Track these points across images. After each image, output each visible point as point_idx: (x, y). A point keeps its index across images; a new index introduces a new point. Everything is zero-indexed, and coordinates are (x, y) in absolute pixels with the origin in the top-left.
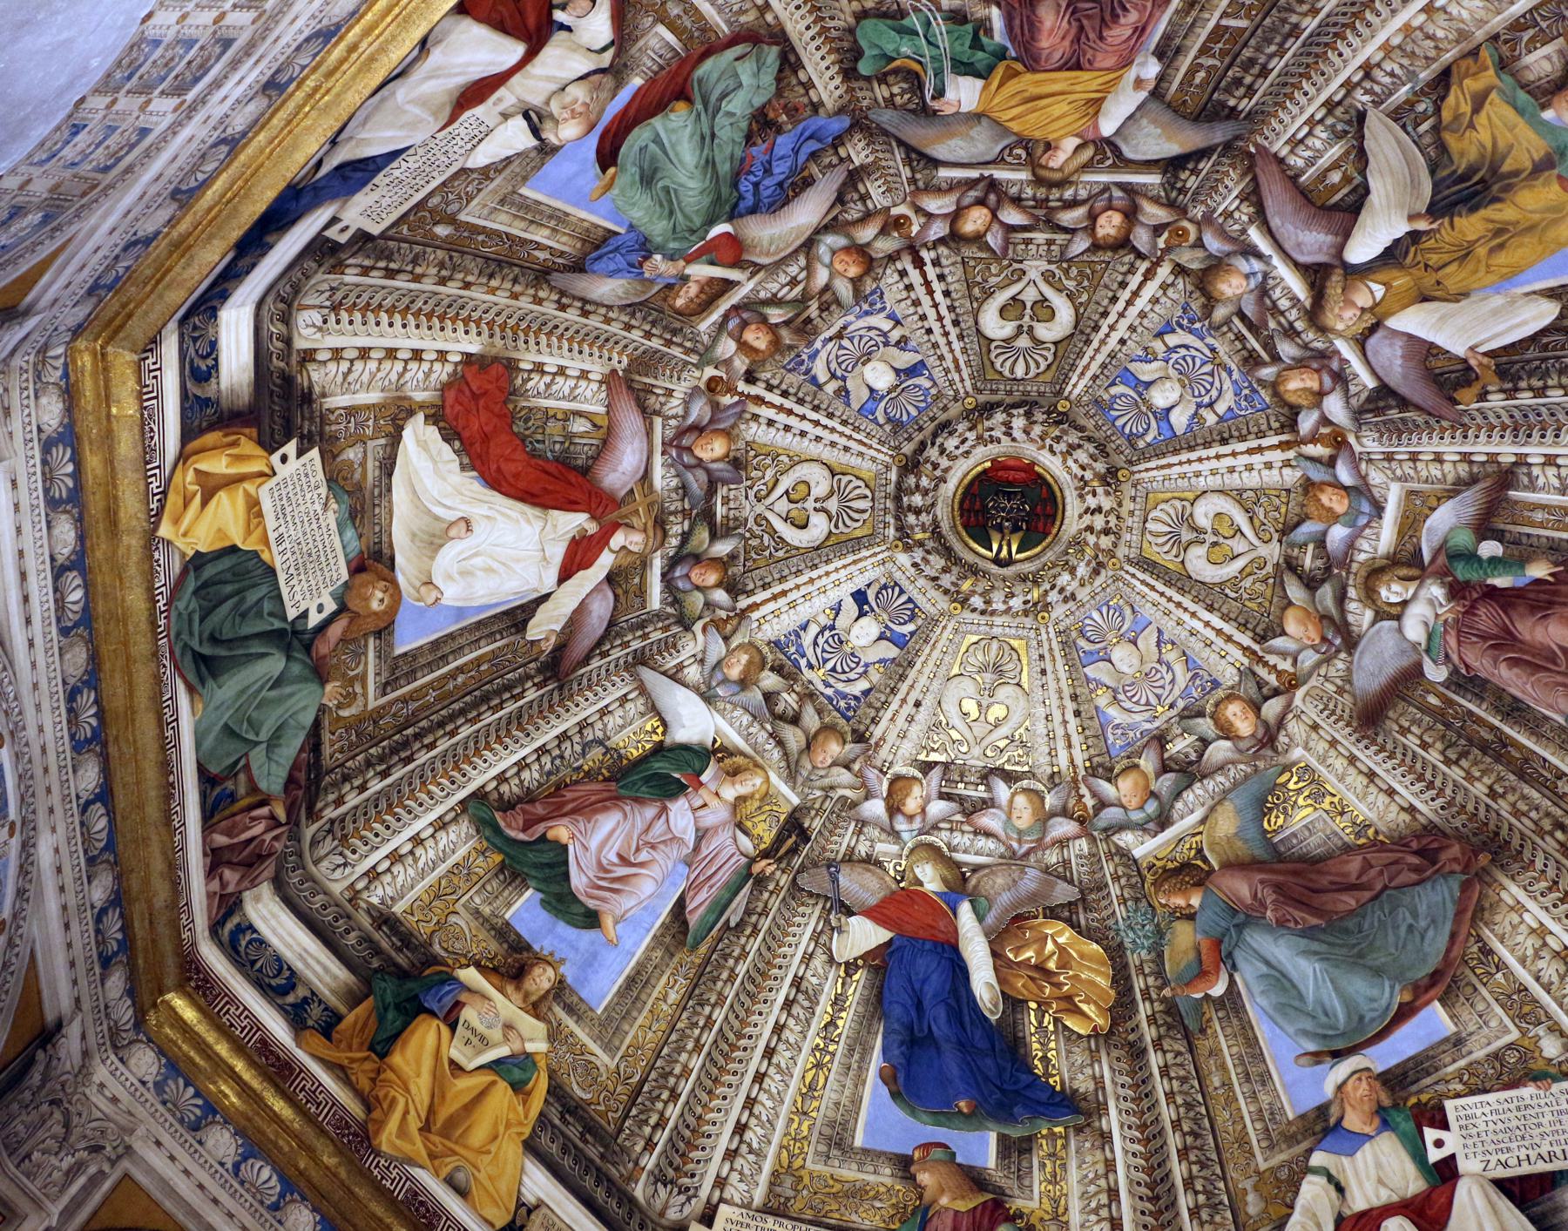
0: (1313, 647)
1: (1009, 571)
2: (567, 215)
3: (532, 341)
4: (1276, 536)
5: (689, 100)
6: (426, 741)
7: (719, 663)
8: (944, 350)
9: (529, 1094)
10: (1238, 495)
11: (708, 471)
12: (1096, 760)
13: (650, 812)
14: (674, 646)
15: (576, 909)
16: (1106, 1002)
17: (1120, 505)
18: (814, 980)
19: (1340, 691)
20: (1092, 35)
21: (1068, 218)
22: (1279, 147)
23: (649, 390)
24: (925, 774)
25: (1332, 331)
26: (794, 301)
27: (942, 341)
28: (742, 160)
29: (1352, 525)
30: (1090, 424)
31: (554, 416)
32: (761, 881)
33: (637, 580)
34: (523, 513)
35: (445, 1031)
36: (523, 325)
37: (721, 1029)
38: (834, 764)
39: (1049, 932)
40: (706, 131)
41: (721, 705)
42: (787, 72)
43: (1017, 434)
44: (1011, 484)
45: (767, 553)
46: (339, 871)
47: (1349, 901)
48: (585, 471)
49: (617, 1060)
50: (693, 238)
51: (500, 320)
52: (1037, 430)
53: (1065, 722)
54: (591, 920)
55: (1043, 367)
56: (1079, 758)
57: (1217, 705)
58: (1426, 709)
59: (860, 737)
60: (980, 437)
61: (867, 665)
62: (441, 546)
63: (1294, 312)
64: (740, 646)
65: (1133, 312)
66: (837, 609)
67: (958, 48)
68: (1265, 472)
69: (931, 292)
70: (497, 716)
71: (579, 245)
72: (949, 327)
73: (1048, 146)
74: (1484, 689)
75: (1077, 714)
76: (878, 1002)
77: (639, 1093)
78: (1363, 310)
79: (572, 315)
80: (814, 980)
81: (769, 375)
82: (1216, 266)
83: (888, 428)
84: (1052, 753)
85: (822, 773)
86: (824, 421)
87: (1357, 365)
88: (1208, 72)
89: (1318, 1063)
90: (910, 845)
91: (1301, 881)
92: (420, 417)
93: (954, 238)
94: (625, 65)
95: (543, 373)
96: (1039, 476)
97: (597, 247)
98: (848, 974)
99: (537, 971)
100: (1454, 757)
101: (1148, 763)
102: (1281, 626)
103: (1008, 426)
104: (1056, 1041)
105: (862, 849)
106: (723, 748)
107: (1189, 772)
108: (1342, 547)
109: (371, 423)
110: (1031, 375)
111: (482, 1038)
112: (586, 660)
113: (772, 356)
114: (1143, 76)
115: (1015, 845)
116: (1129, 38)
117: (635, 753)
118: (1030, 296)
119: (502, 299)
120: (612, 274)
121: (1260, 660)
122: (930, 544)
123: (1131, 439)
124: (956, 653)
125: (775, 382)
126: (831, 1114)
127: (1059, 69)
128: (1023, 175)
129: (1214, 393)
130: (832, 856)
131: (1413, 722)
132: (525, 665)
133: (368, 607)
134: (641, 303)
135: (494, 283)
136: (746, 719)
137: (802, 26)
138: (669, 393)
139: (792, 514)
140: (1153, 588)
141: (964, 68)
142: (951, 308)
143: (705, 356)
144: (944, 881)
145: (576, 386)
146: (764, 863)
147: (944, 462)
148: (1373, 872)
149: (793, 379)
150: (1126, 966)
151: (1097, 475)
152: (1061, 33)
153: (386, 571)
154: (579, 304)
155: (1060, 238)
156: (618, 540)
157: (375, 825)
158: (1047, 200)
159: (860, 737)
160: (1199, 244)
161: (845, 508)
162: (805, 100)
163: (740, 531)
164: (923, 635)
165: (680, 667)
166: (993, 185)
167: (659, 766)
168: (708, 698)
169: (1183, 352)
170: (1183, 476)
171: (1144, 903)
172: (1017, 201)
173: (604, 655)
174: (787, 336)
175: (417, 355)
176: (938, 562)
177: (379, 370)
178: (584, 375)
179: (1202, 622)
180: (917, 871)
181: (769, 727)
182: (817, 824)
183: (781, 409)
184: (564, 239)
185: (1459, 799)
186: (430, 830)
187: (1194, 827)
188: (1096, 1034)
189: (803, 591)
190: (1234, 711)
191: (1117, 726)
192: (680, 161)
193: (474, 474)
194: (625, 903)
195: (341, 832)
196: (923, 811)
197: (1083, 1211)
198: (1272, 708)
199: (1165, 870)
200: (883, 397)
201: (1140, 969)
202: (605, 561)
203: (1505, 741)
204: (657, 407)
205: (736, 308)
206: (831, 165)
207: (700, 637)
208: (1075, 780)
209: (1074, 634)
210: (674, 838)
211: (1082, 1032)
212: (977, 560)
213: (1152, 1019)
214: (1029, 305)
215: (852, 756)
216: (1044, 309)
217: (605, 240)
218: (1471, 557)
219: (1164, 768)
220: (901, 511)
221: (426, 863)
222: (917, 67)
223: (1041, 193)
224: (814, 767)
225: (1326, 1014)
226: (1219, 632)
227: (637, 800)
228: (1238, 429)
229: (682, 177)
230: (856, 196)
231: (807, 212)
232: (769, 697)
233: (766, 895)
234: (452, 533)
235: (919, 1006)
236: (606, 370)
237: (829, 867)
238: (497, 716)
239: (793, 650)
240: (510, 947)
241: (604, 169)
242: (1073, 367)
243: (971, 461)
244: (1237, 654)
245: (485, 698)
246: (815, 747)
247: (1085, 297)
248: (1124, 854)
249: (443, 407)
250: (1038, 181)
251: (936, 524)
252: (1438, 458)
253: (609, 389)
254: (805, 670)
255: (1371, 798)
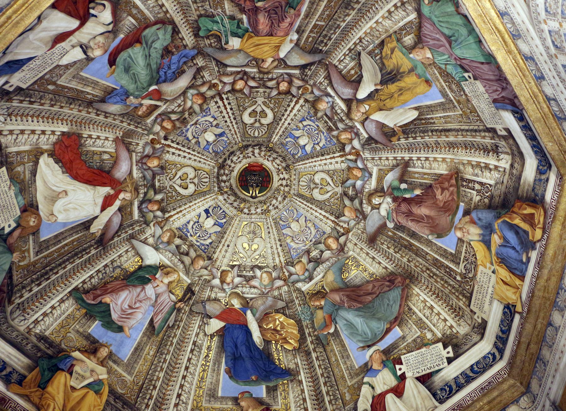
0: (353, 219)
1: (256, 200)
2: (98, 82)
3: (87, 127)
4: (340, 185)
5: (141, 43)
6: (55, 271)
7: (160, 236)
8: (231, 128)
9: (102, 394)
10: (328, 172)
11: (152, 171)
12: (288, 260)
13: (139, 289)
14: (144, 231)
15: (114, 326)
16: (297, 338)
17: (291, 177)
18: (200, 342)
19: (363, 233)
20: (276, 25)
21: (271, 84)
22: (335, 62)
23: (130, 143)
24: (232, 269)
25: (354, 120)
26: (180, 112)
27: (230, 125)
28: (160, 64)
29: (363, 180)
30: (280, 151)
31: (96, 153)
32: (179, 310)
33: (129, 210)
34: (87, 188)
35: (68, 376)
36: (84, 121)
37: (169, 362)
38: (201, 268)
39: (277, 317)
40: (147, 54)
41: (161, 251)
42: (175, 34)
43: (256, 155)
44: (255, 171)
46: (23, 322)
47: (369, 298)
48: (109, 172)
49: (133, 377)
50: (144, 91)
51: (75, 120)
52: (263, 153)
53: (277, 248)
54: (120, 329)
55: (264, 132)
56: (283, 260)
57: (325, 239)
58: (388, 236)
59: (210, 258)
60: (244, 156)
61: (210, 234)
62: (56, 201)
63: (342, 114)
64: (167, 230)
65: (292, 114)
66: (199, 216)
67: (233, 28)
68: (336, 165)
69: (226, 109)
70: (81, 260)
71: (103, 93)
72: (233, 120)
73: (263, 61)
74: (404, 229)
75: (281, 245)
76: (222, 347)
77: (142, 388)
78: (363, 113)
79: (101, 118)
80: (200, 342)
81: (172, 137)
82: (318, 100)
83: (213, 154)
84: (274, 259)
85: (197, 271)
86: (192, 152)
87: (362, 130)
88: (313, 38)
89: (364, 350)
90: (229, 293)
91: (354, 293)
92: (46, 155)
93: (233, 91)
94: (117, 30)
95: (92, 138)
96: (264, 168)
97: (110, 94)
98: (212, 339)
99: (102, 350)
100: (397, 251)
101: (305, 260)
102: (343, 213)
103: (253, 152)
104: (282, 353)
105: (213, 296)
106: (163, 266)
107: (318, 262)
108: (361, 187)
109: (26, 157)
110: (260, 135)
111: (83, 376)
112: (113, 238)
114: (293, 39)
115: (264, 290)
116: (288, 26)
117: (132, 270)
118: (259, 109)
119: (75, 112)
120: (115, 103)
121: (338, 224)
122: (229, 192)
123: (293, 155)
124: (240, 228)
125: (174, 140)
126: (210, 386)
127: (266, 36)
128: (255, 70)
129: (319, 140)
130: (203, 299)
131: (385, 241)
132: (90, 242)
133: (29, 224)
134: (126, 113)
135: (72, 106)
136: (170, 255)
137: (179, 19)
138: (138, 144)
139: (182, 184)
140: (303, 203)
141: (235, 35)
142: (233, 114)
143: (150, 131)
144: (241, 304)
145: (104, 143)
146: (180, 303)
147: (233, 165)
148: (376, 289)
149: (180, 139)
150: (302, 326)
151: (283, 167)
152: (266, 24)
153: (35, 211)
154: (104, 114)
155: (268, 90)
156: (122, 196)
157: (36, 304)
158: (263, 78)
159: (210, 258)
160: (312, 92)
161: (200, 181)
162: (181, 44)
164: (229, 223)
165: (146, 239)
166: (245, 73)
167: (141, 273)
168: (157, 249)
169: (309, 127)
170: (310, 167)
171: (307, 305)
172: (253, 78)
173: (119, 236)
174: (178, 124)
175: (43, 132)
176: (232, 198)
177: (28, 138)
178: (107, 139)
179: (318, 214)
180: (232, 302)
181: (178, 257)
182: (197, 289)
183: (177, 149)
184: (97, 91)
185: (399, 263)
186: (58, 303)
187: (320, 279)
188: (295, 349)
189: (187, 210)
190: (331, 241)
191: (294, 249)
192: (138, 64)
193: (67, 174)
194: (132, 322)
195: (23, 308)
196: (233, 281)
197: (295, 407)
198: (342, 239)
199: (312, 294)
200: (211, 144)
201: (307, 326)
202: (118, 203)
203: (411, 245)
204: (133, 149)
205: (160, 115)
206: (191, 66)
207: (153, 228)
208: (282, 267)
209: (278, 220)
210: (148, 298)
211: (290, 349)
212: (246, 197)
213: (312, 342)
214: (258, 112)
215: (207, 265)
216: (263, 114)
217: (112, 91)
218: (398, 189)
219: (310, 261)
220: (219, 182)
221: (57, 316)
222: (219, 34)
223: (261, 76)
224: (195, 270)
225: (365, 334)
226: (324, 216)
227: (134, 286)
228: (327, 151)
229: (139, 70)
230: (200, 77)
231: (183, 82)
232: (178, 247)
233: (181, 314)
234: (60, 196)
235: (236, 346)
236: (115, 137)
237: (202, 303)
238: (81, 260)
239: (185, 230)
240: (91, 342)
241: (111, 66)
242: (274, 132)
243: (242, 164)
244: (330, 223)
245: (76, 254)
246: (195, 263)
247: (276, 110)
248: (299, 290)
249: (54, 151)
250: (260, 72)
251: (231, 185)
252: (387, 159)
253: (116, 143)
254: (190, 237)
255: (374, 265)
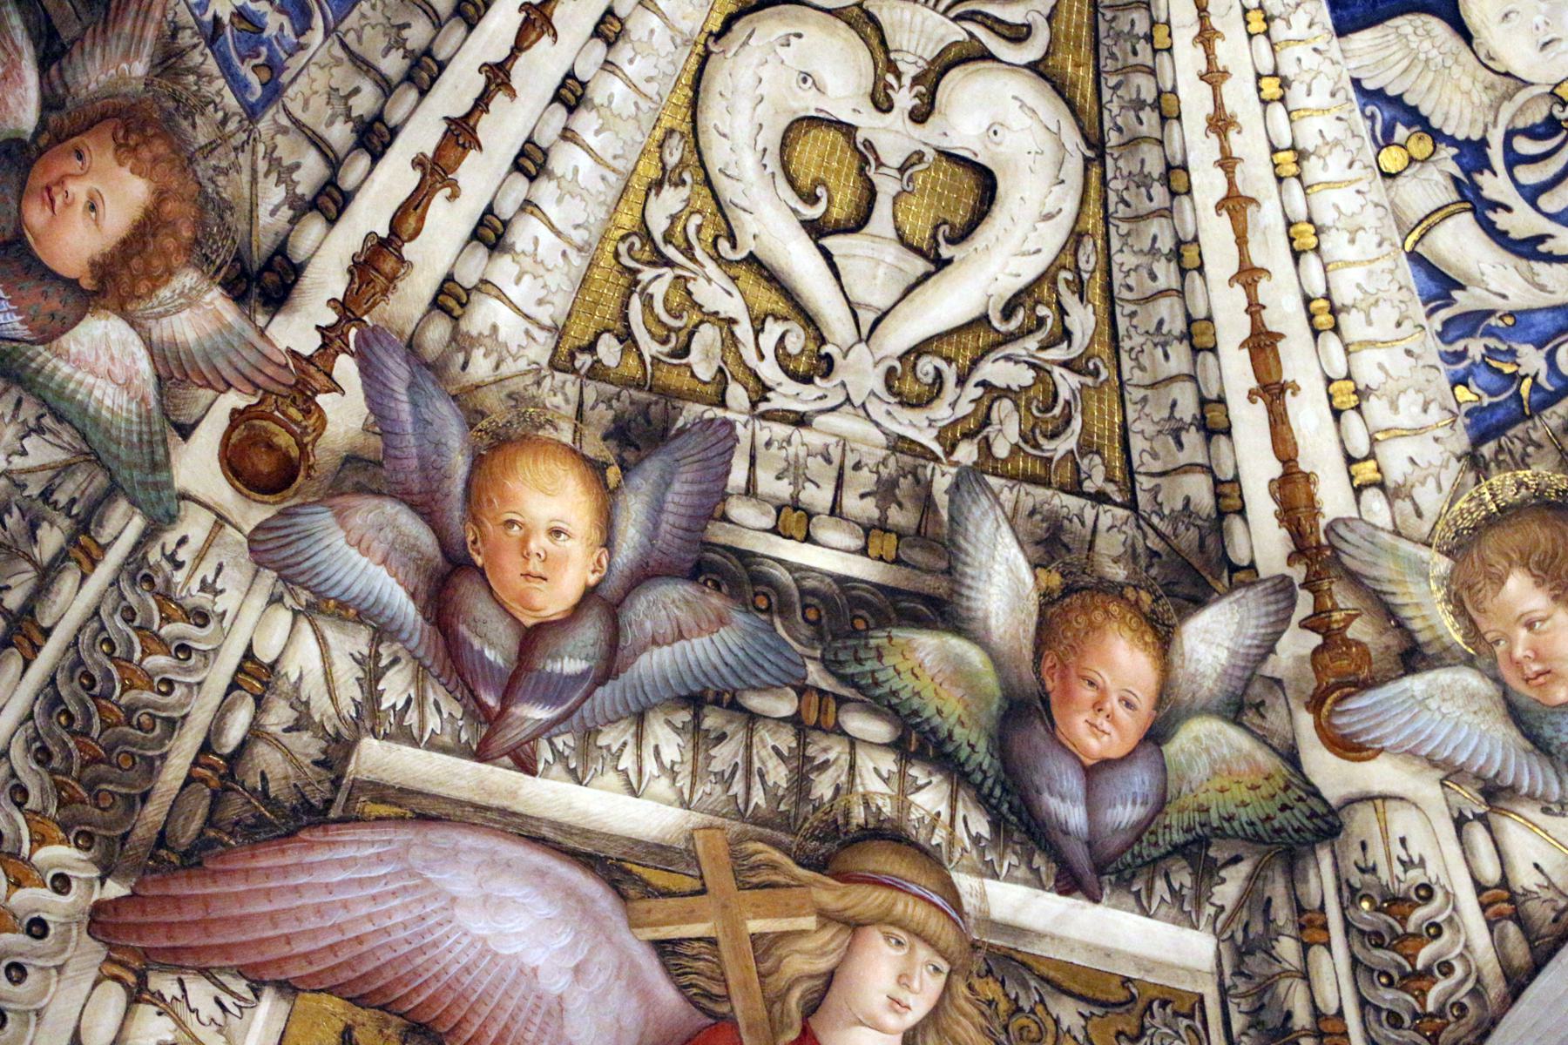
7: (1516, 713)
11: (645, 574)
14: (1395, 903)
45: (1067, 383)
81: (273, 194)
113: (185, 158)
125: (311, 172)
139: (919, 229)
163: (941, 484)
189: (1270, 251)
204: (308, 746)
207: (1379, 774)
236: (88, 954)
239: (1532, 360)
253: (176, 960)
